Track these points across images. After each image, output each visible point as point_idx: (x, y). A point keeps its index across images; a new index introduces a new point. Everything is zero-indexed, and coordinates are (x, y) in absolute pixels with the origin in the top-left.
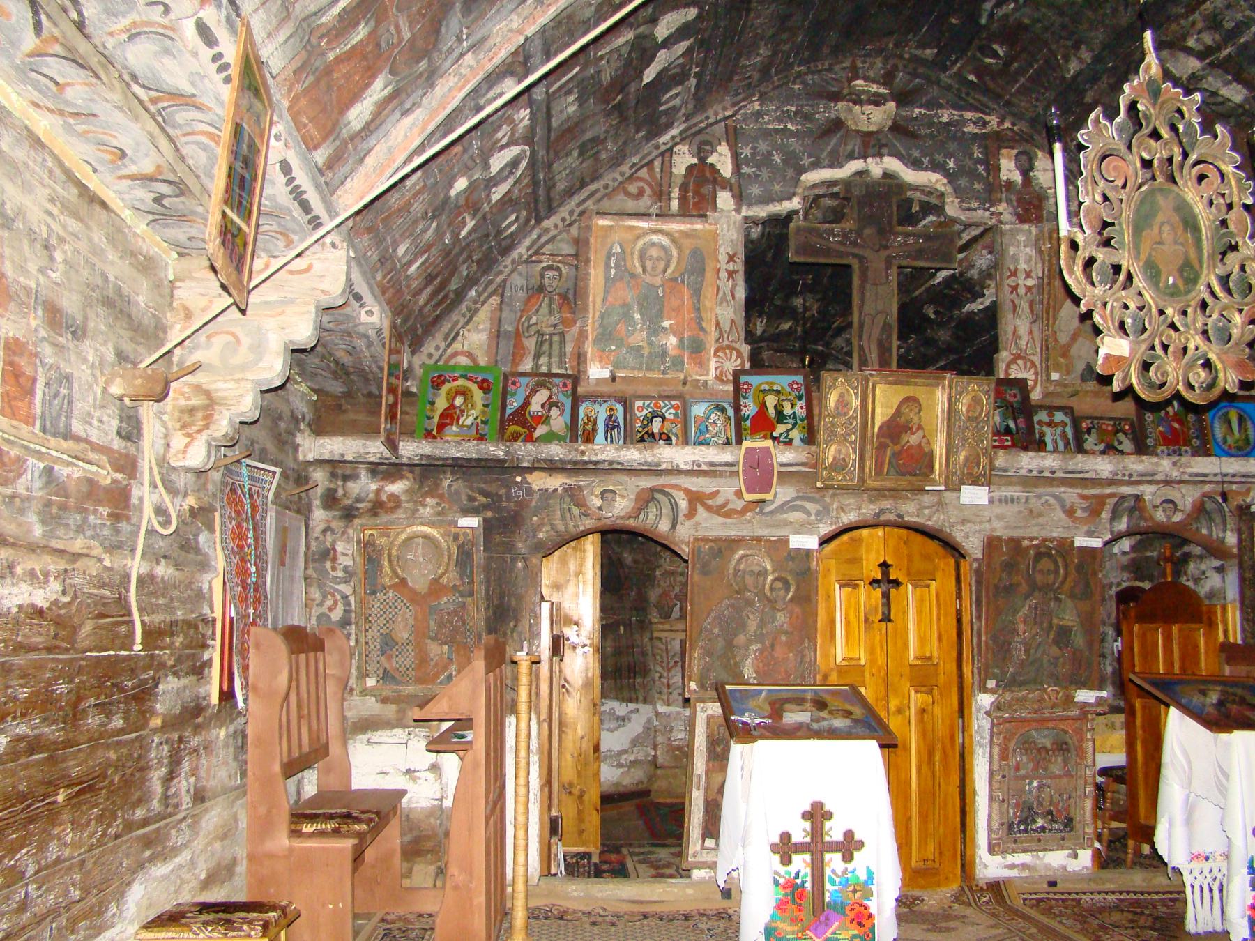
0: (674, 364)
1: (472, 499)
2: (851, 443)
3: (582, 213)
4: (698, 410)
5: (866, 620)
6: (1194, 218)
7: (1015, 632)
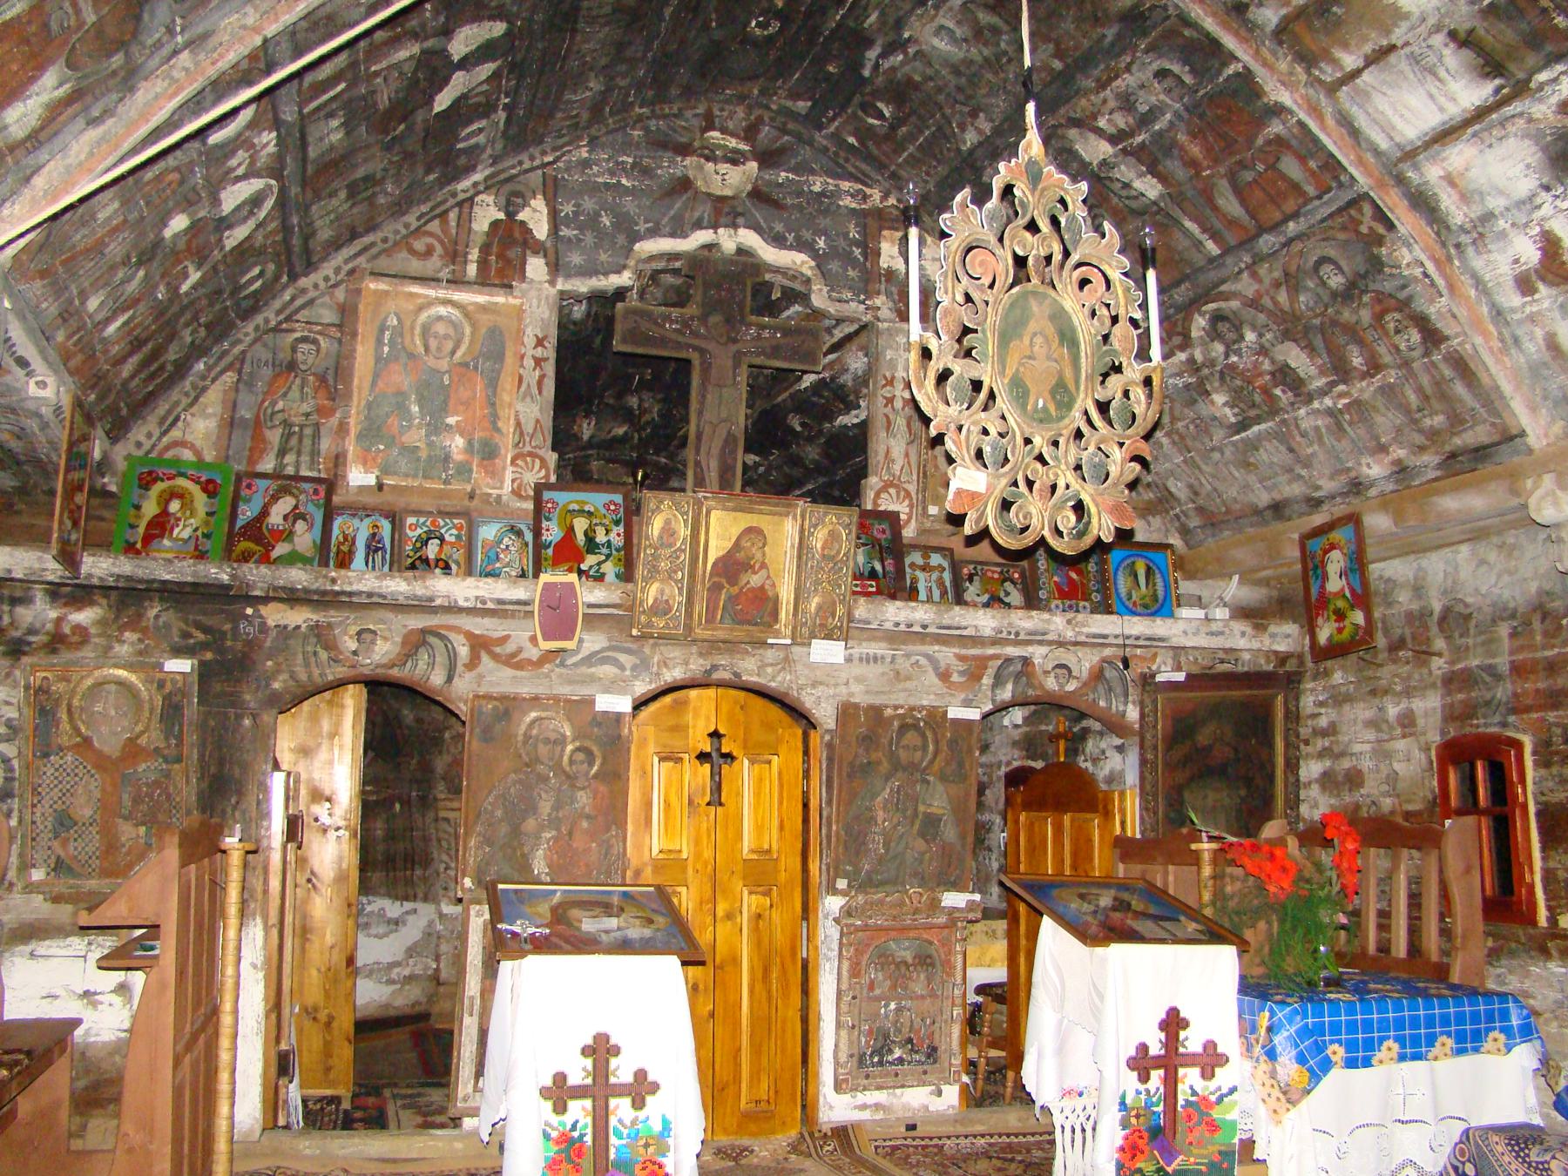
0: (459, 472)
1: (186, 635)
2: (676, 581)
3: (352, 272)
4: (488, 532)
5: (691, 802)
6: (1073, 330)
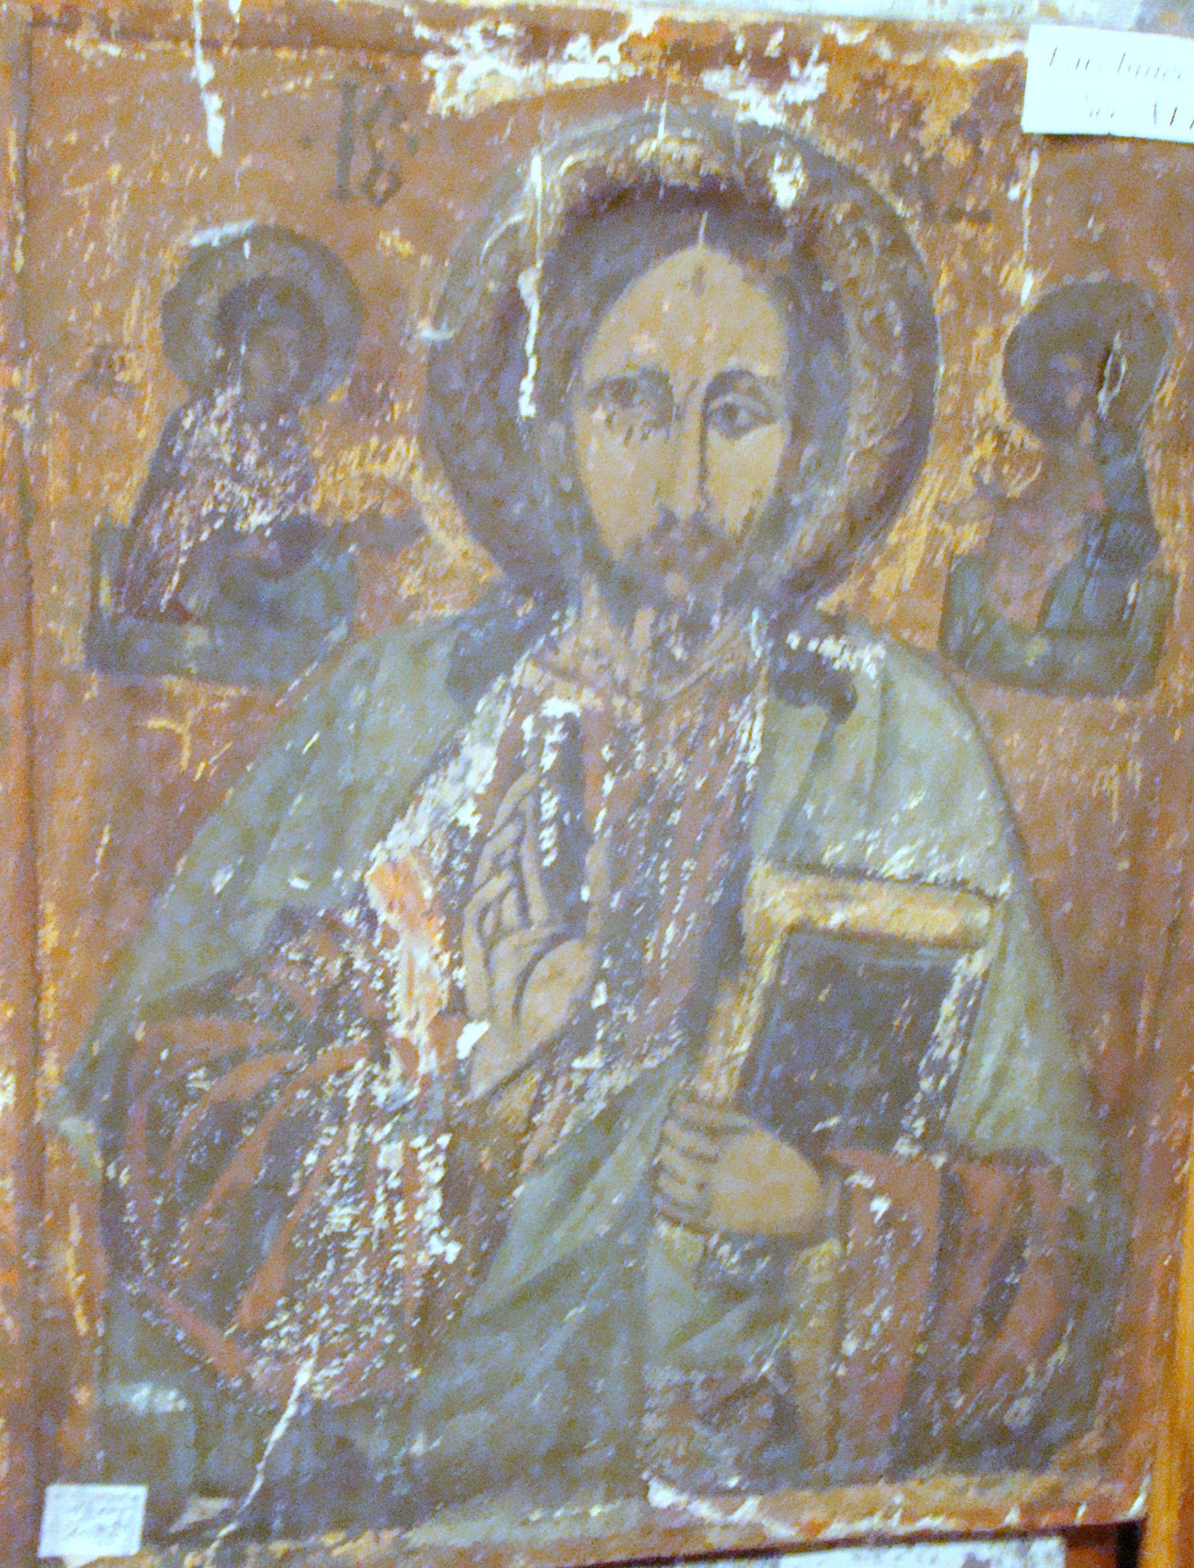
7: (350, 1012)
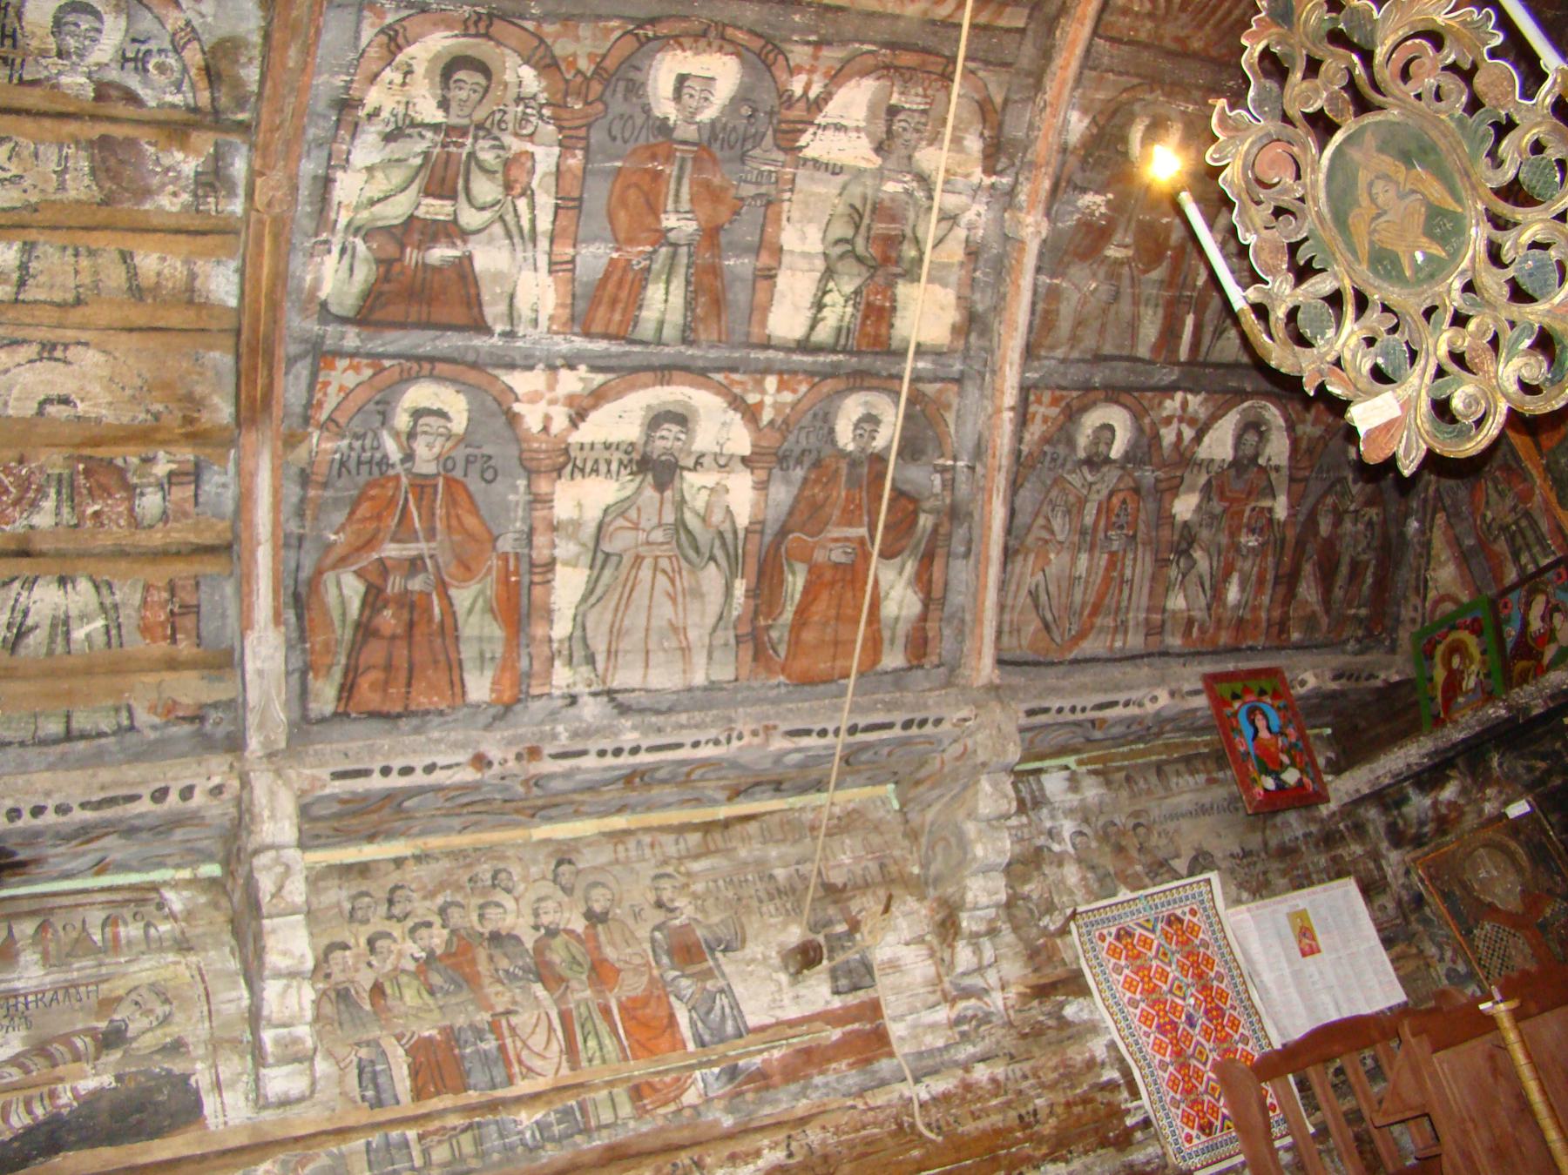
1: (1530, 769)
